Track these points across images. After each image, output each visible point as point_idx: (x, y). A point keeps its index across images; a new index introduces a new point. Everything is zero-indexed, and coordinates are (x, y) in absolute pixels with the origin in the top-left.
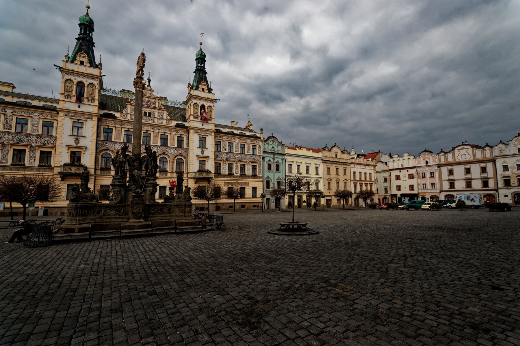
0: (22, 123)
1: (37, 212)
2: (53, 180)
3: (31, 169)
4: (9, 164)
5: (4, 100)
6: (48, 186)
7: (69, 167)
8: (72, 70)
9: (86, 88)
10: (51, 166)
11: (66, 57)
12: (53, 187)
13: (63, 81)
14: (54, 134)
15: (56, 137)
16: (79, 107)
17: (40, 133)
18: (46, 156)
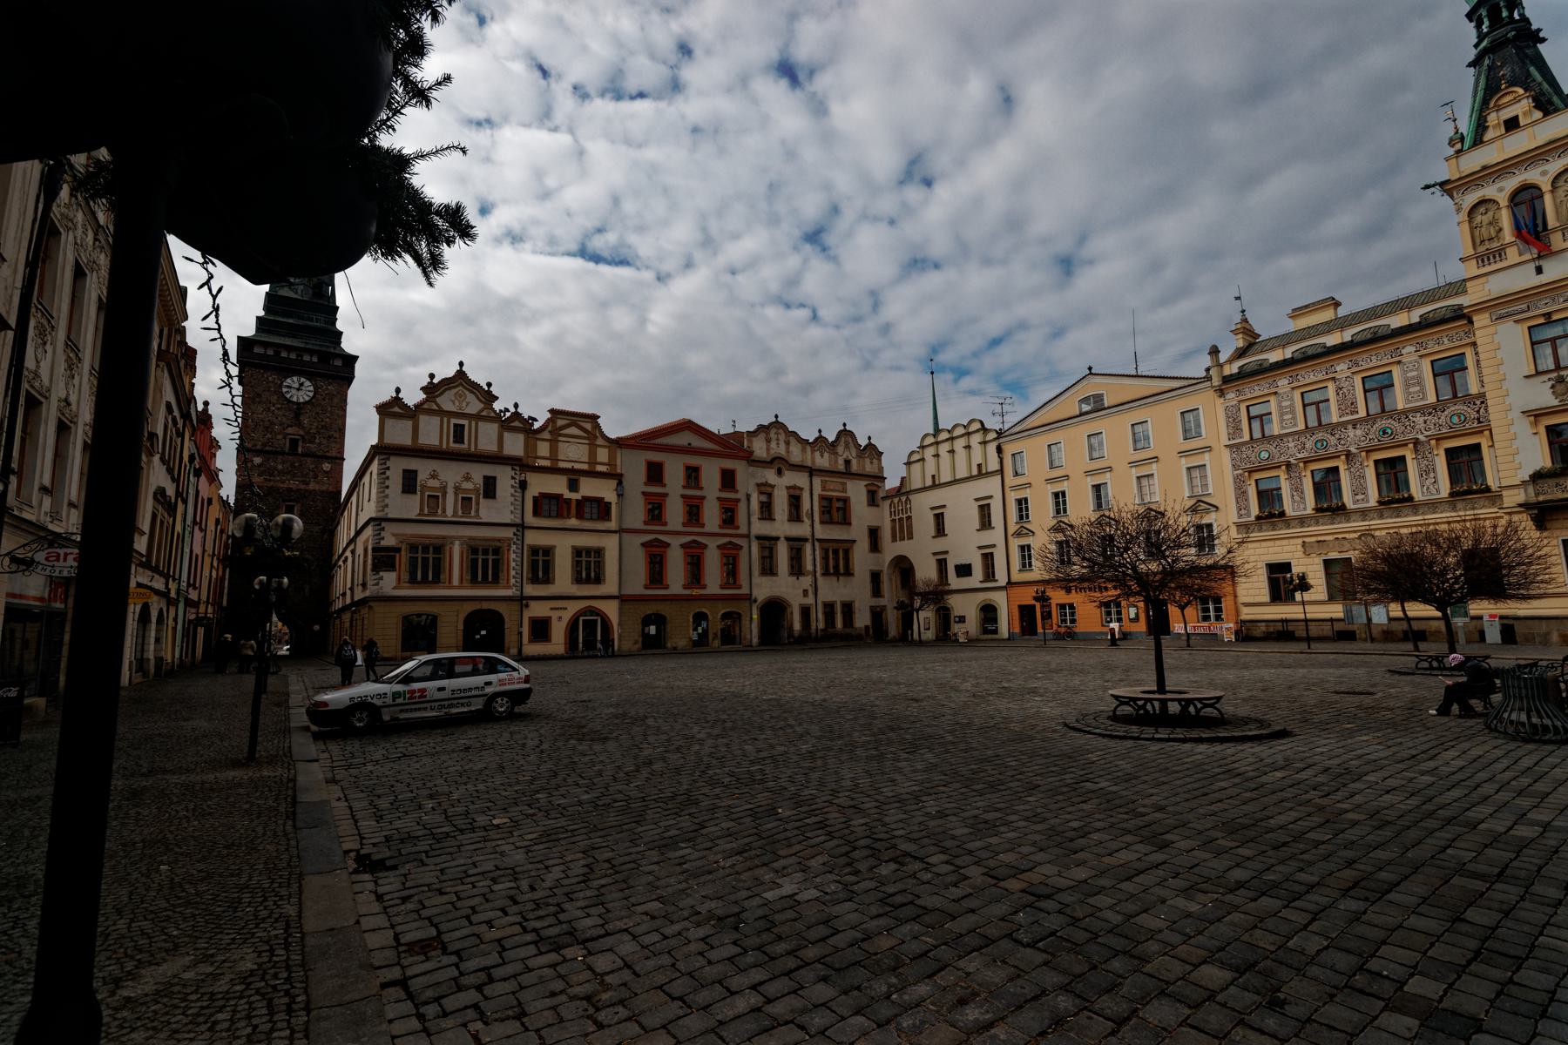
0: (1379, 386)
1: (1482, 634)
2: (1512, 529)
3: (1433, 505)
4: (1373, 503)
5: (1324, 346)
6: (1497, 550)
7: (1552, 482)
8: (1485, 168)
9: (1548, 198)
10: (1488, 489)
11: (1451, 143)
12: (1519, 552)
13: (1464, 216)
14: (1474, 389)
15: (1482, 396)
16: (1539, 270)
17: (1432, 399)
18: (1465, 462)
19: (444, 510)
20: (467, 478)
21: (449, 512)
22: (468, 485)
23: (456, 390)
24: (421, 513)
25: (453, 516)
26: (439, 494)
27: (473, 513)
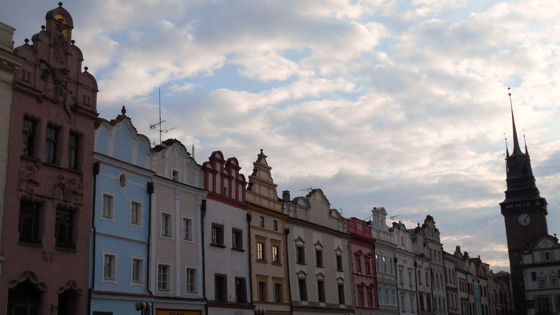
19: (547, 285)
20: (553, 272)
21: (549, 285)
22: (554, 275)
23: (544, 240)
24: (539, 287)
25: (550, 287)
26: (544, 280)
27: (557, 284)
